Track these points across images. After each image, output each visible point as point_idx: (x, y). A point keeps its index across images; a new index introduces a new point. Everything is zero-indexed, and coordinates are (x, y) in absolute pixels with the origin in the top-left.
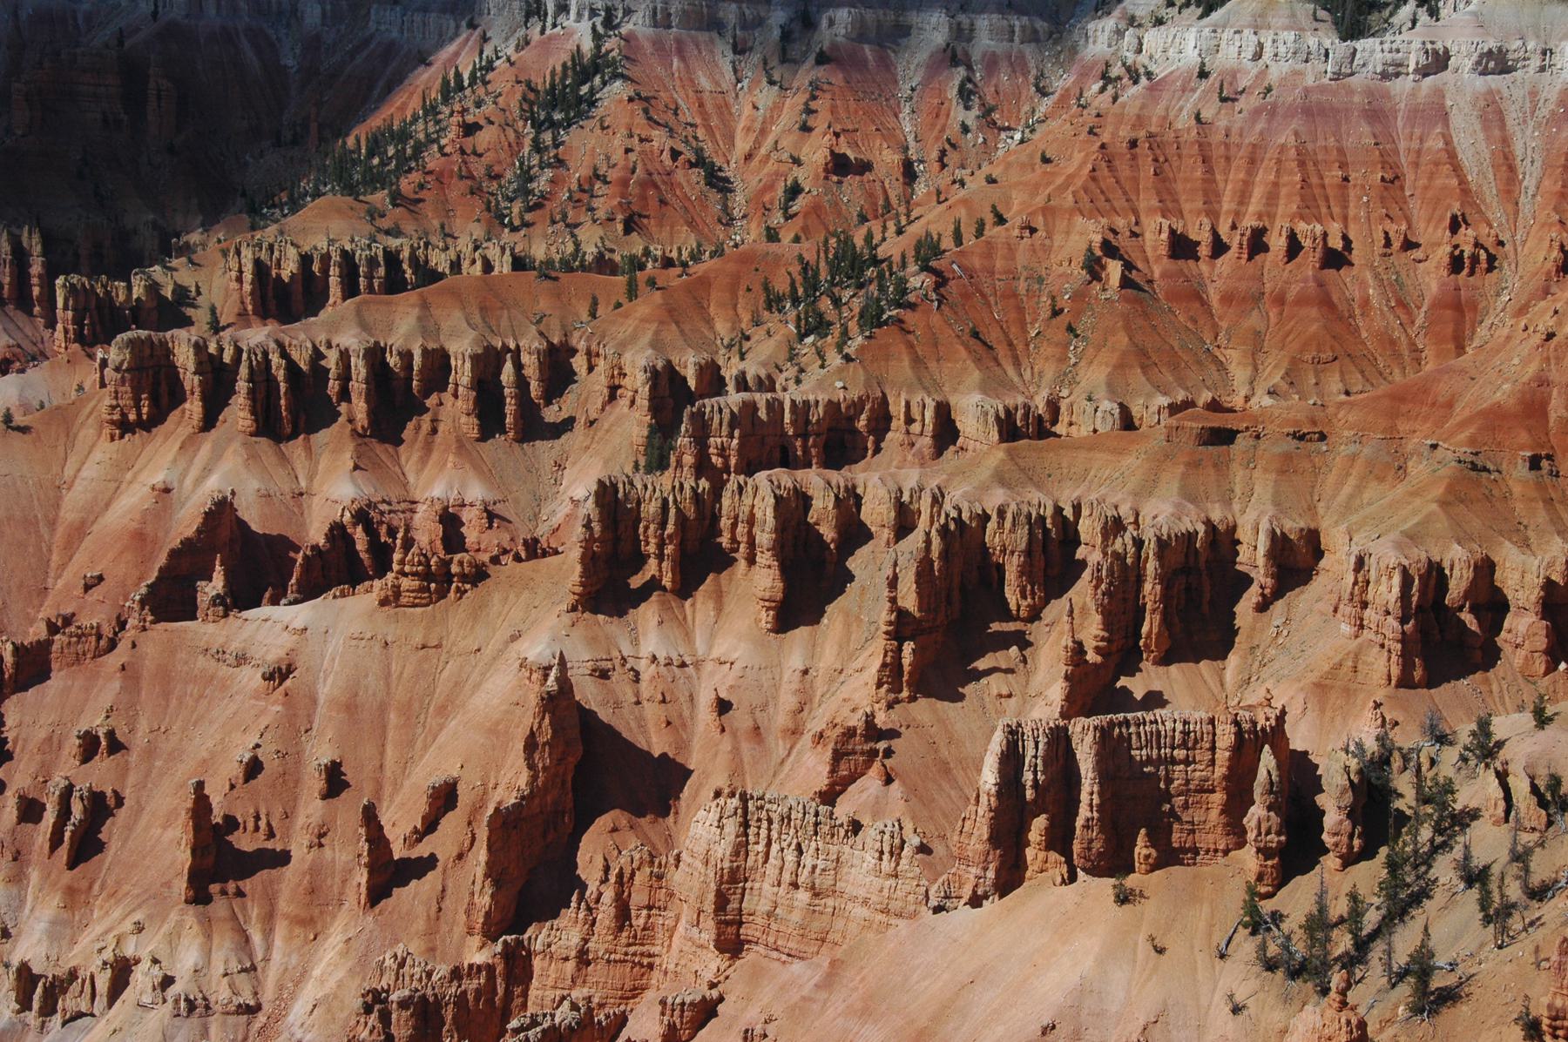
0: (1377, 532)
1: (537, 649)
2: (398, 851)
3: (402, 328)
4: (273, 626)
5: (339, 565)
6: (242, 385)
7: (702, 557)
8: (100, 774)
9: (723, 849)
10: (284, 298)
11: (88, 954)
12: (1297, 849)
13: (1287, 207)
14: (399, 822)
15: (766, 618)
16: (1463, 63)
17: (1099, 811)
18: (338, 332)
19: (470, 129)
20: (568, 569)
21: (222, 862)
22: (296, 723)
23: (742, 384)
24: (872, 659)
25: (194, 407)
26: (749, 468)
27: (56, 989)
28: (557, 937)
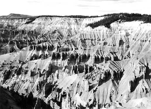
0: (93, 54)
1: (49, 62)
2: (42, 73)
3: (44, 44)
4: (35, 61)
5: (40, 57)
6: (36, 48)
7: (59, 56)
8: (26, 69)
9: (57, 73)
10: (39, 43)
11: (25, 79)
12: (86, 72)
13: (90, 37)
14: (41, 72)
15: (62, 60)
16: (98, 30)
17: (78, 70)
18: (41, 45)
19: (49, 34)
20: (51, 57)
21: (33, 74)
22: (36, 67)
23: (62, 47)
24: (67, 62)
25: (33, 49)
26: (62, 51)
27: (24, 81)
28: (49, 78)
